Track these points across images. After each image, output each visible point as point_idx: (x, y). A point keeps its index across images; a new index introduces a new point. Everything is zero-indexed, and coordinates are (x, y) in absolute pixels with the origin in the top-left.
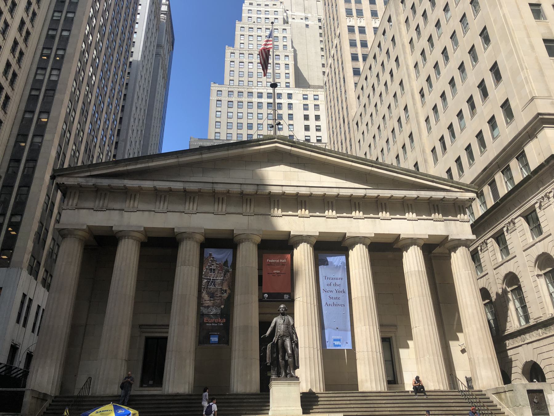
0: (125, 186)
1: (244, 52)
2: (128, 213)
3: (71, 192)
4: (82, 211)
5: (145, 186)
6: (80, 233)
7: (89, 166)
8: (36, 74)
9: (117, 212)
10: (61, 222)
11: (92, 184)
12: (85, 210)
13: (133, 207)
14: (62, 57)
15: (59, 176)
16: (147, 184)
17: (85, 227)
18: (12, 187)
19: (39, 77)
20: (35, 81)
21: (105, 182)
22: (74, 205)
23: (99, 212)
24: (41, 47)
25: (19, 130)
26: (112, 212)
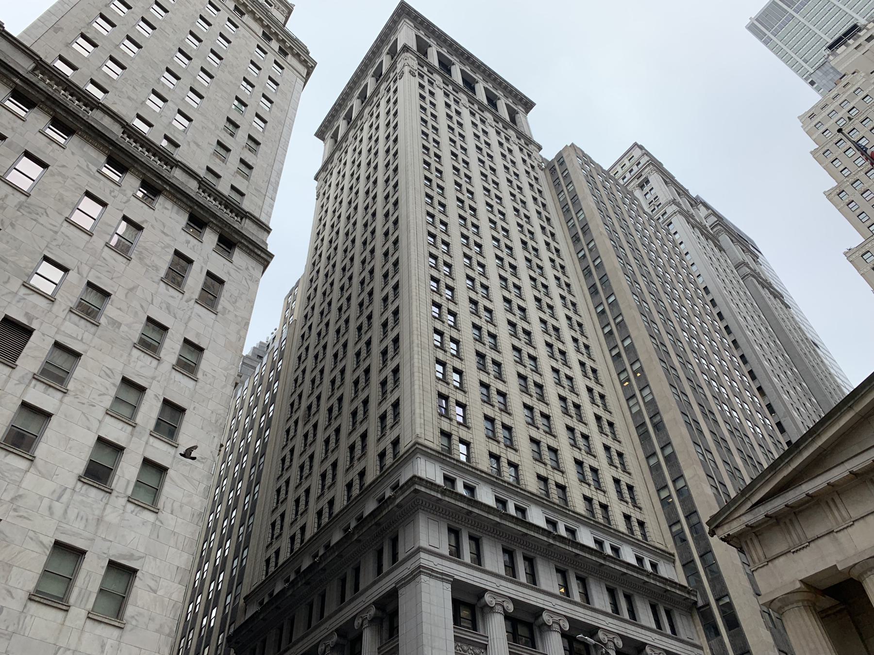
0: (807, 495)
1: (857, 177)
2: (842, 533)
3: (746, 542)
4: (776, 562)
5: (837, 478)
6: (798, 597)
7: (728, 505)
8: (630, 408)
9: (826, 538)
10: (762, 593)
11: (762, 517)
12: (782, 559)
13: (844, 520)
14: (641, 369)
15: (717, 527)
16: (837, 474)
17: (798, 585)
18: (693, 561)
19: (635, 410)
20: (634, 416)
21: (777, 504)
22: (763, 558)
23: (802, 552)
24: (615, 375)
25: (655, 484)
26: (820, 541)
